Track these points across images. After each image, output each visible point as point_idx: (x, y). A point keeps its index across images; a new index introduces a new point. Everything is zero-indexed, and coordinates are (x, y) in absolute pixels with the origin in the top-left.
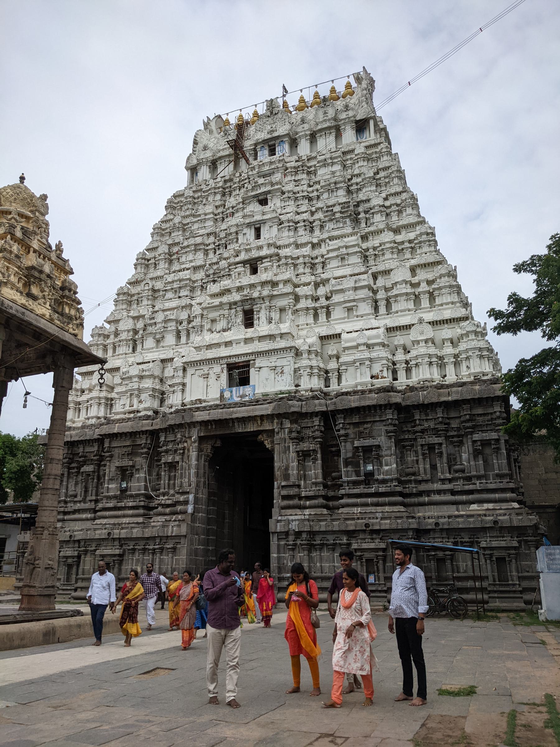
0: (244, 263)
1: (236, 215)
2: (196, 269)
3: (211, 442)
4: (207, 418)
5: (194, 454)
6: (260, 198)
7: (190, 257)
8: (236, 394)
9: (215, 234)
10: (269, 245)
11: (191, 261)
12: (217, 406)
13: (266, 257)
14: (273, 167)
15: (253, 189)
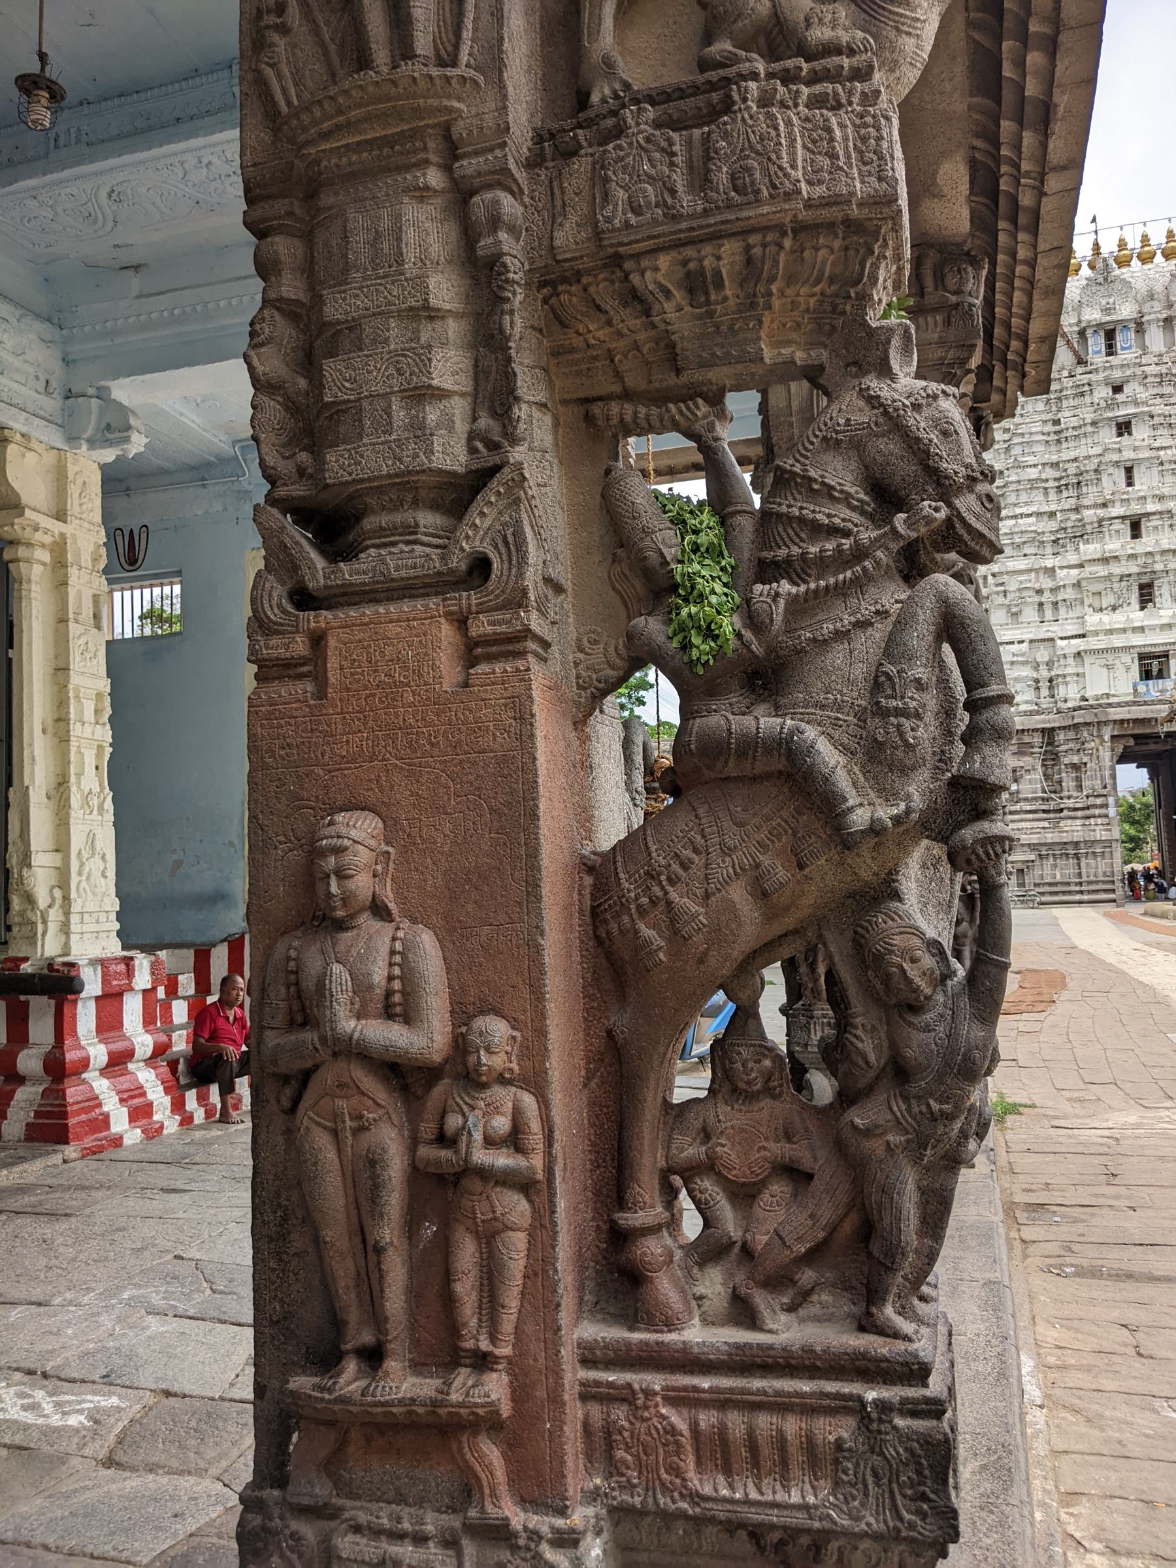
0: (1123, 518)
1: (1083, 441)
2: (1039, 514)
3: (1124, 741)
4: (1128, 716)
5: (1108, 754)
6: (1121, 420)
7: (1024, 497)
8: (1153, 689)
9: (1055, 465)
10: (1155, 496)
11: (1027, 503)
12: (1135, 703)
13: (1154, 514)
14: (1128, 373)
15: (1108, 407)
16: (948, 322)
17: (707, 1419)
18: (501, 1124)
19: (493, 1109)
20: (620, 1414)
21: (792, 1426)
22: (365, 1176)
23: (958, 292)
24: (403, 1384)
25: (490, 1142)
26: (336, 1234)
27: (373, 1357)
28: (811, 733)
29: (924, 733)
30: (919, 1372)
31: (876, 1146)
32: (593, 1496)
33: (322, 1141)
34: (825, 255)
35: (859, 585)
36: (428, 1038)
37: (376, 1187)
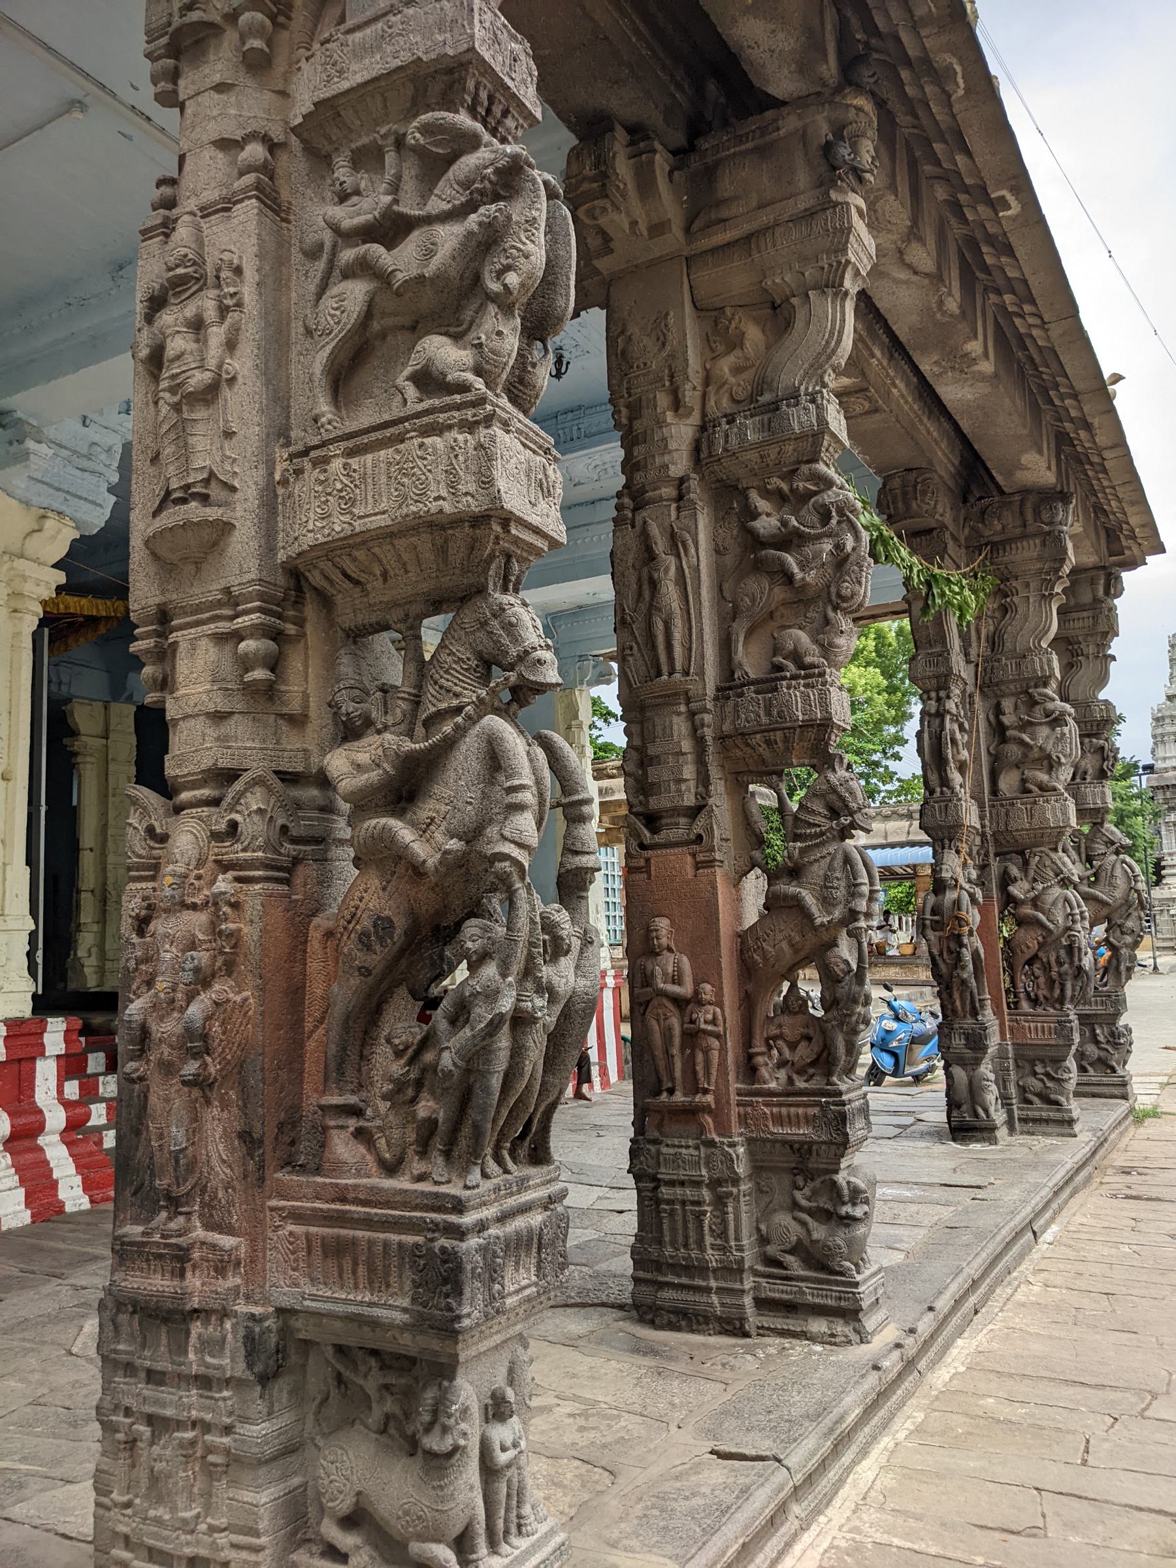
16: (1044, 544)
17: (775, 1110)
18: (710, 1017)
19: (707, 1012)
20: (749, 1109)
21: (801, 1111)
22: (667, 1034)
23: (1050, 523)
24: (679, 1097)
25: (706, 1022)
26: (659, 1053)
27: (671, 1092)
28: (804, 893)
29: (840, 894)
30: (840, 1094)
31: (829, 1025)
32: (741, 1134)
33: (654, 1023)
34: (811, 734)
35: (823, 843)
36: (686, 990)
37: (671, 1037)
